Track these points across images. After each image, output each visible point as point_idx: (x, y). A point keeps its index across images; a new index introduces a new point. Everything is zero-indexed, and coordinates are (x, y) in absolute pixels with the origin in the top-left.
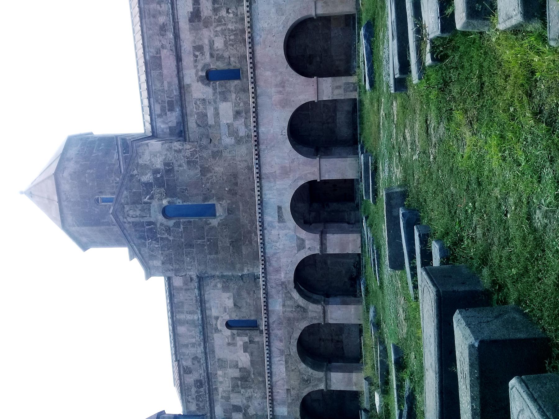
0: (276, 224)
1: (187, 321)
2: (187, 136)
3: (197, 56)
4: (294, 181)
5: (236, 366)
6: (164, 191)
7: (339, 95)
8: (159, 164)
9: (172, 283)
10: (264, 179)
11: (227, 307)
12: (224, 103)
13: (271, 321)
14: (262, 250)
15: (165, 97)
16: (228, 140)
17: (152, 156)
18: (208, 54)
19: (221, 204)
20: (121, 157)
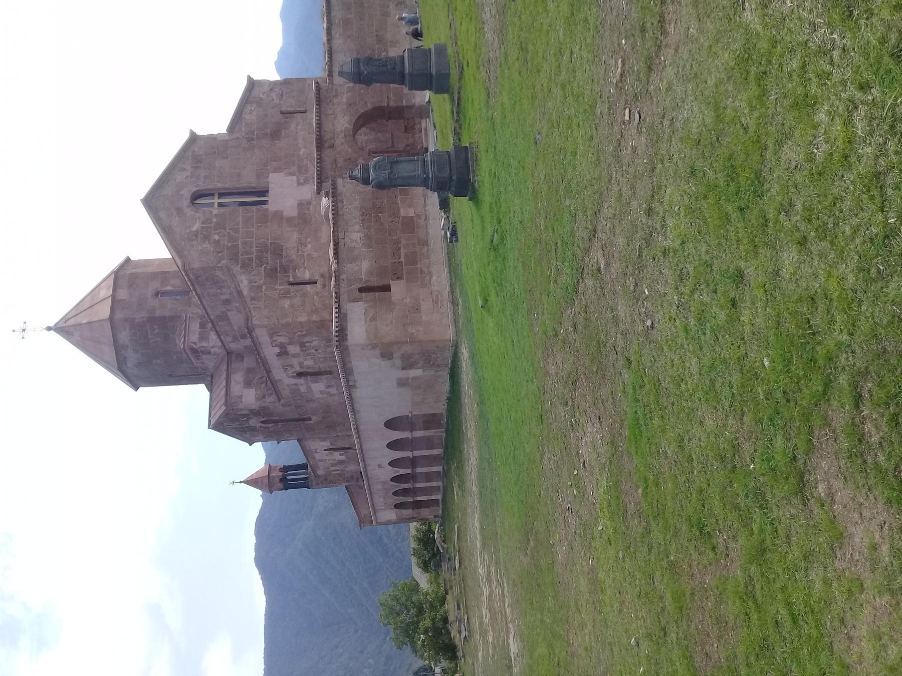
5: (335, 460)
12: (317, 384)
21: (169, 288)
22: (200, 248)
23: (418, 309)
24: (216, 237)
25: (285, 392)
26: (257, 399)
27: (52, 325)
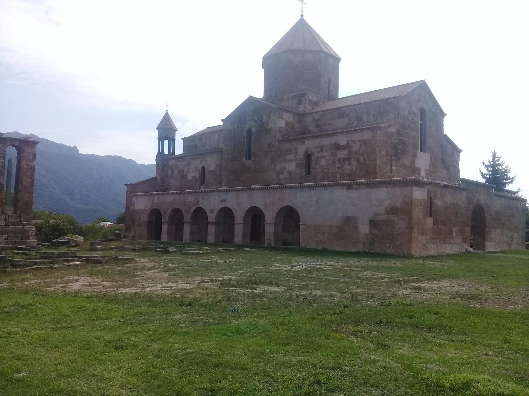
0: (219, 199)
3: (318, 148)
5: (188, 172)
7: (267, 236)
8: (271, 125)
10: (237, 192)
16: (279, 166)
18: (318, 155)
20: (296, 93)
21: (332, 88)
22: (406, 108)
23: (423, 234)
24: (410, 119)
25: (287, 145)
26: (280, 128)
27: (304, 18)
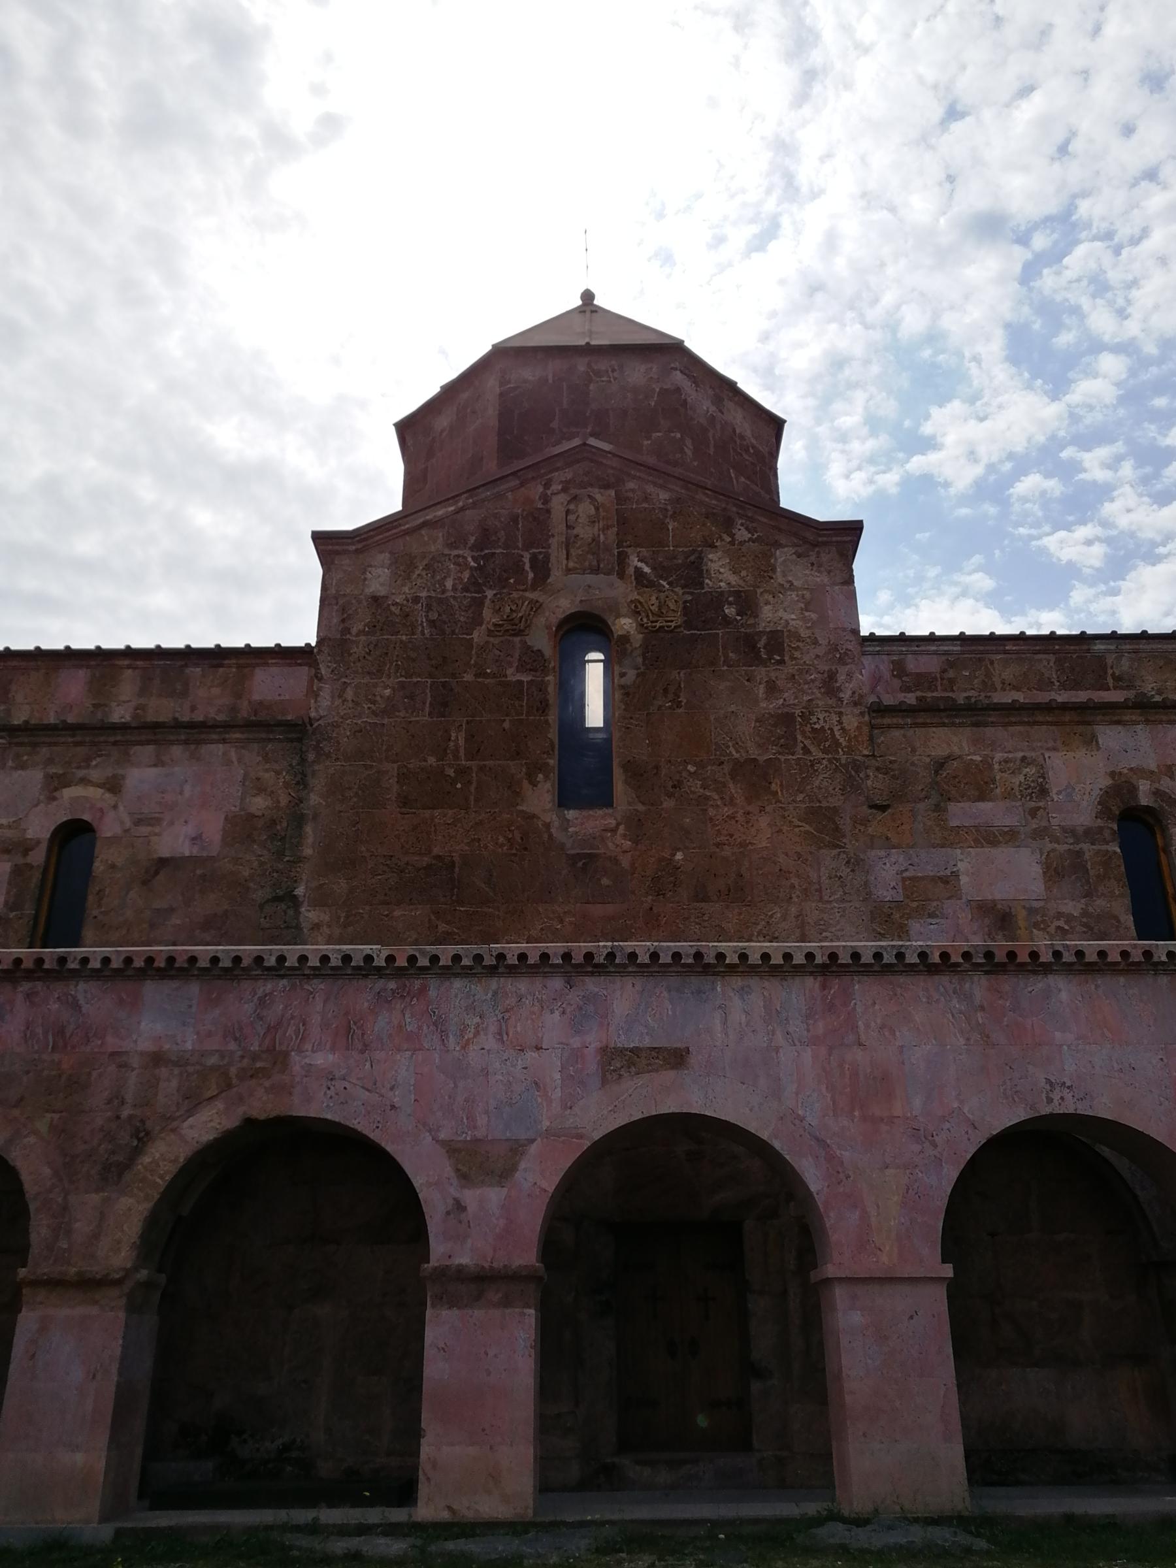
0: (593, 1039)
1: (105, 705)
2: (895, 721)
4: (817, 1139)
6: (673, 624)
9: (267, 664)
10: (824, 987)
11: (157, 830)
12: (1036, 870)
13: (81, 990)
14: (466, 962)
15: (965, 690)
17: (808, 595)
19: (614, 831)
